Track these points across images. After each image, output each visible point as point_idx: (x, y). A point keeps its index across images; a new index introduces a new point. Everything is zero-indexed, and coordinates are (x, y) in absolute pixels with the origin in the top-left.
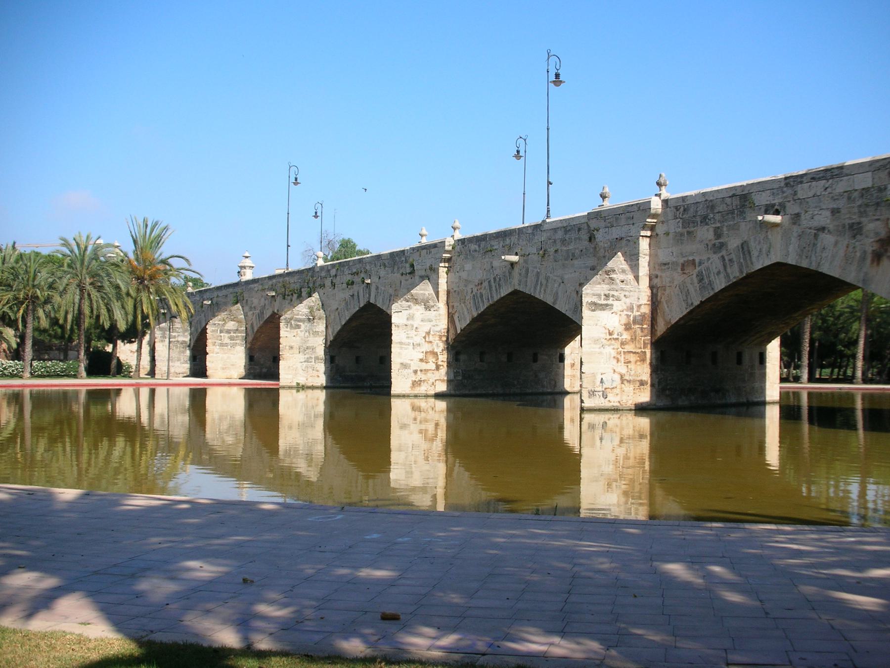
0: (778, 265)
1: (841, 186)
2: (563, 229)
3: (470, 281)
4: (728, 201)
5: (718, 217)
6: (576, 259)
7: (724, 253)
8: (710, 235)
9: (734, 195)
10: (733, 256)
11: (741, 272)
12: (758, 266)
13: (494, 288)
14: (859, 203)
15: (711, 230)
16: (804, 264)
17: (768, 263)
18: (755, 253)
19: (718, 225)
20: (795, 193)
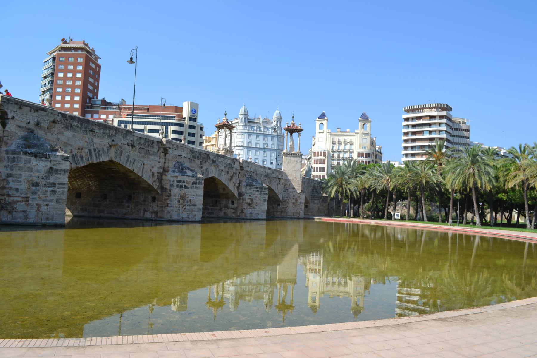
0: (212, 177)
1: (226, 161)
2: (144, 140)
3: (69, 145)
4: (204, 154)
5: (201, 158)
6: (151, 155)
7: (202, 170)
8: (199, 163)
9: (205, 153)
10: (204, 171)
11: (206, 177)
12: (210, 176)
13: (94, 155)
14: (228, 166)
15: (200, 162)
16: (219, 178)
17: (212, 176)
18: (209, 172)
19: (201, 161)
20: (218, 159)
